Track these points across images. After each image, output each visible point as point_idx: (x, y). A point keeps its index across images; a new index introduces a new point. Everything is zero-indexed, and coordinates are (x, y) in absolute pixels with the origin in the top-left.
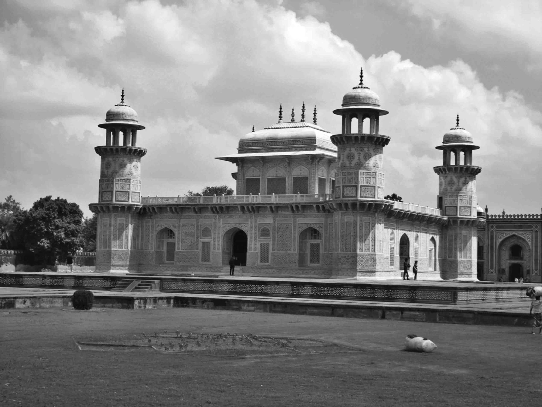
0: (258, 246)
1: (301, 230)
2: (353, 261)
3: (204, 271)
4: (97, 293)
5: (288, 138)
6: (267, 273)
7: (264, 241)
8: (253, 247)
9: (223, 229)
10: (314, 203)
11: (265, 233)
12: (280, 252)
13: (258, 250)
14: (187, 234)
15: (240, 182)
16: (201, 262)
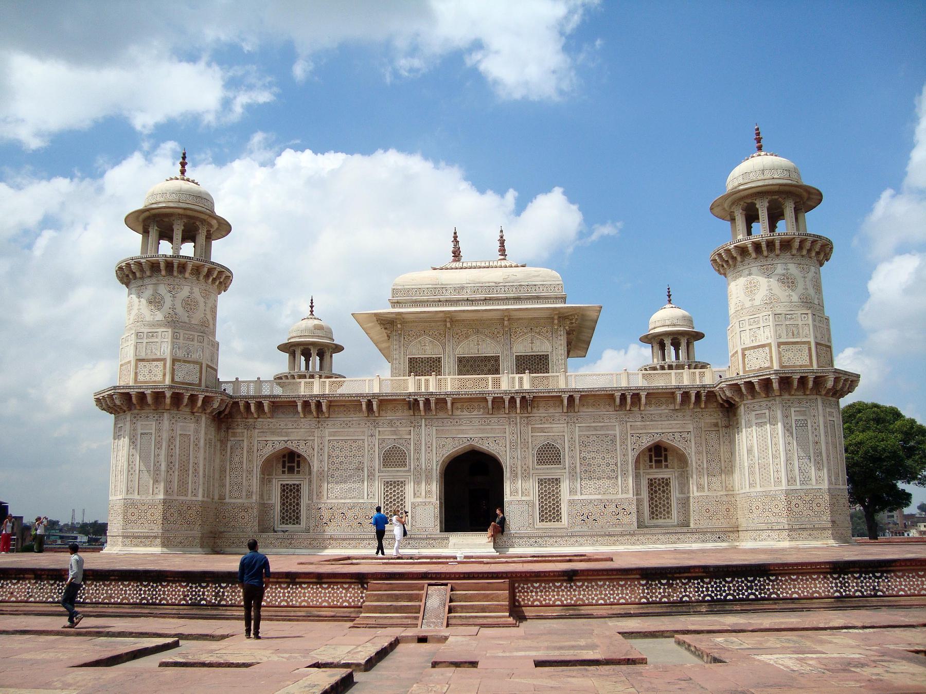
7: (550, 471)
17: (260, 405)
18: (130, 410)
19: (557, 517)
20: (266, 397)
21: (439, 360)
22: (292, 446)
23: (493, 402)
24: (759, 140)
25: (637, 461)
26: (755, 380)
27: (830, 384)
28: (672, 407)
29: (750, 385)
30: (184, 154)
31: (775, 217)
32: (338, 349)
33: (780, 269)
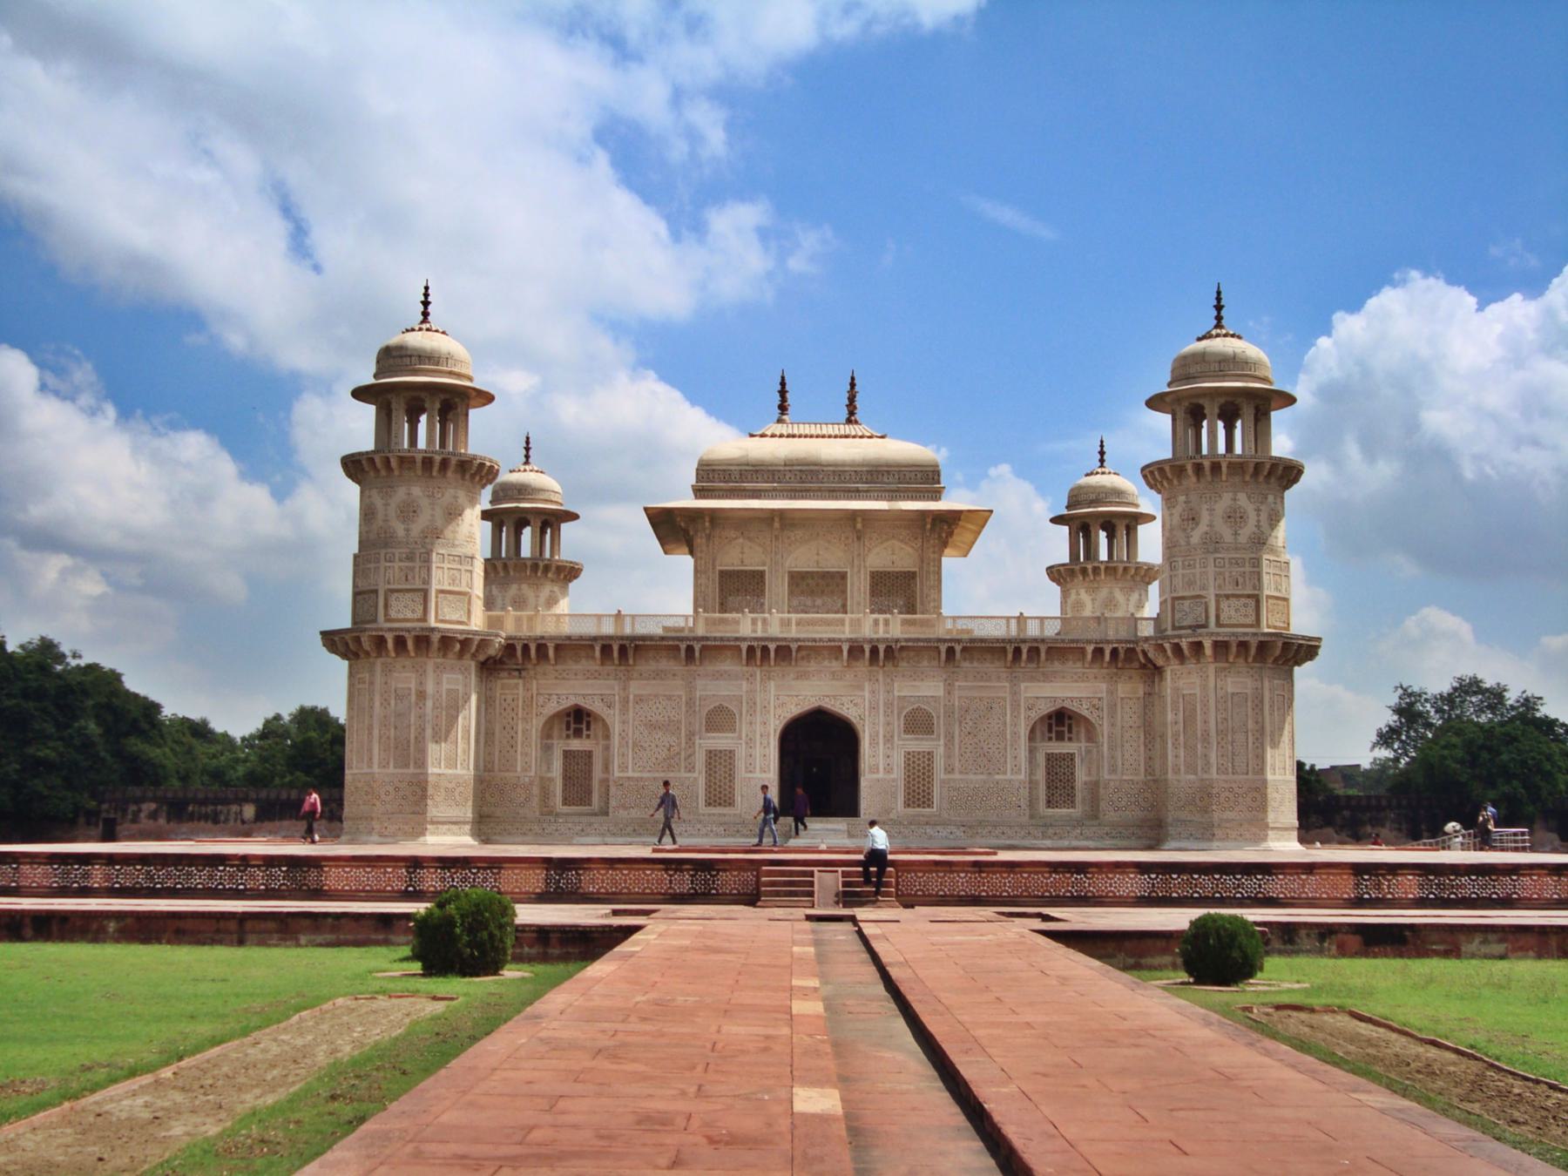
0: (898, 760)
1: (1035, 715)
2: (1254, 800)
3: (717, 835)
4: (529, 914)
5: (853, 464)
6: (930, 837)
8: (880, 765)
9: (779, 711)
10: (865, 640)
11: (918, 723)
12: (971, 777)
13: (898, 774)
14: (653, 726)
15: (703, 581)
16: (702, 808)
17: (542, 648)
18: (379, 655)
19: (927, 801)
20: (552, 638)
21: (762, 574)
22: (586, 704)
23: (850, 651)
24: (1219, 308)
25: (1032, 731)
26: (1184, 644)
27: (1278, 652)
28: (1079, 664)
29: (1177, 649)
30: (427, 288)
31: (1229, 418)
32: (572, 516)
33: (1227, 498)
